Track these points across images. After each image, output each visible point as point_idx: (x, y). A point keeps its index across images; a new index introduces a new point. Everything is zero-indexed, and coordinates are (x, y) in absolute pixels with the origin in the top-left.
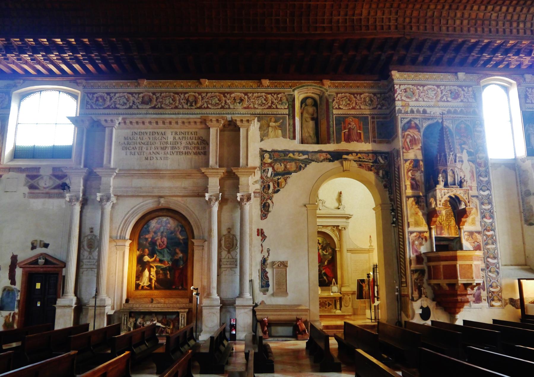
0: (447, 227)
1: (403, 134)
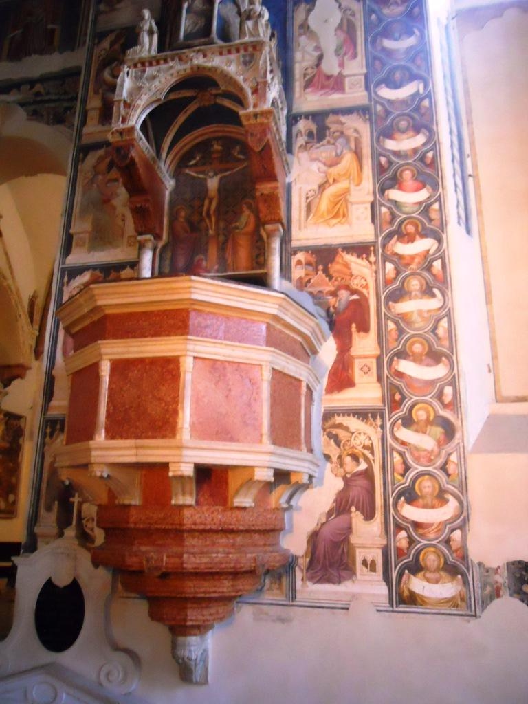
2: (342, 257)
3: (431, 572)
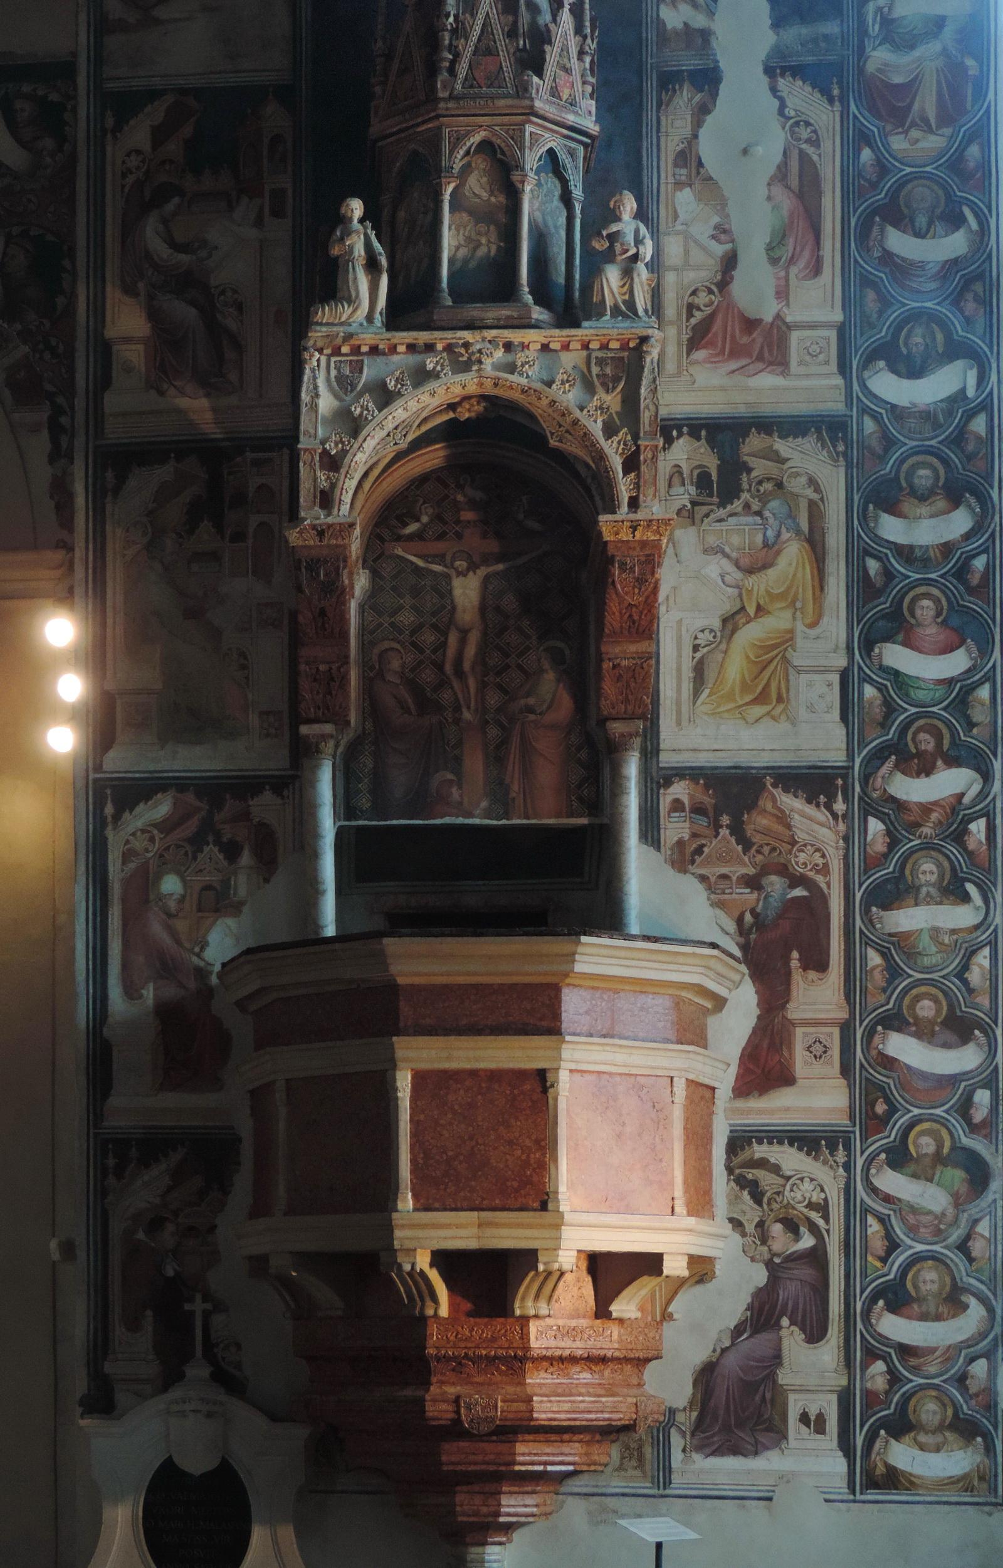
2: (774, 800)
3: (927, 1433)
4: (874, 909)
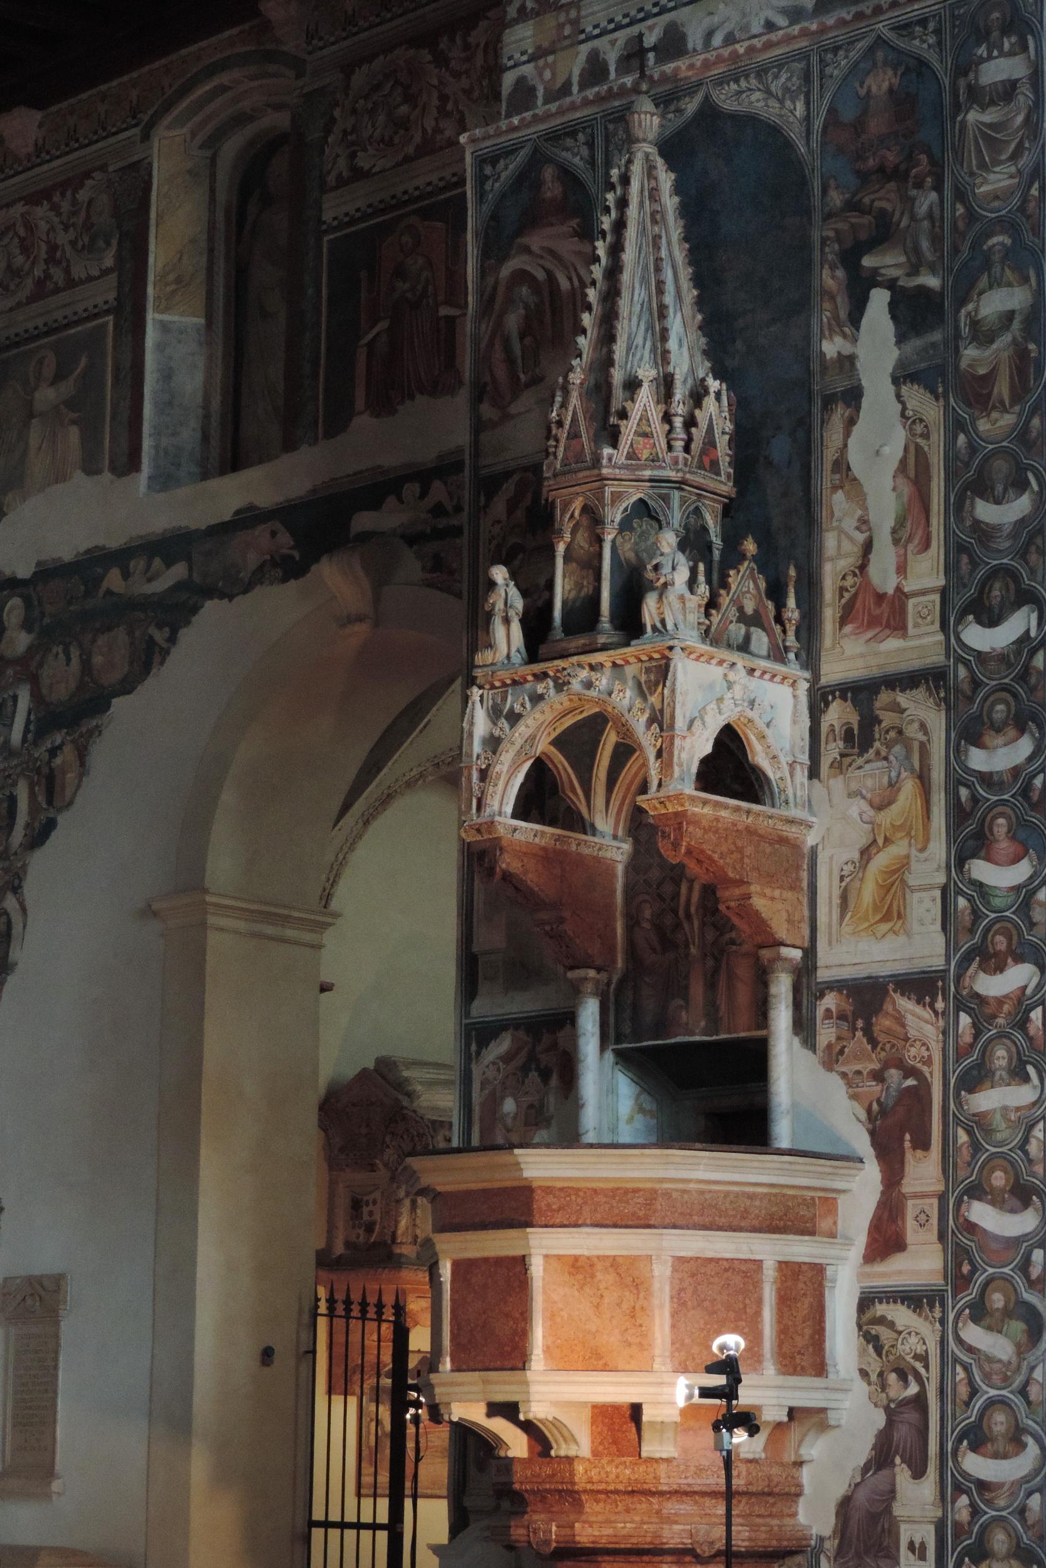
0: (710, 962)
1: (490, 280)
2: (894, 1003)
4: (963, 1093)
